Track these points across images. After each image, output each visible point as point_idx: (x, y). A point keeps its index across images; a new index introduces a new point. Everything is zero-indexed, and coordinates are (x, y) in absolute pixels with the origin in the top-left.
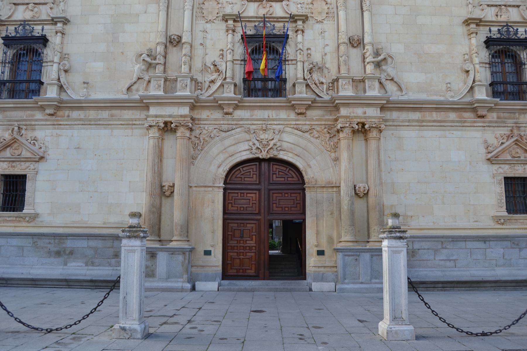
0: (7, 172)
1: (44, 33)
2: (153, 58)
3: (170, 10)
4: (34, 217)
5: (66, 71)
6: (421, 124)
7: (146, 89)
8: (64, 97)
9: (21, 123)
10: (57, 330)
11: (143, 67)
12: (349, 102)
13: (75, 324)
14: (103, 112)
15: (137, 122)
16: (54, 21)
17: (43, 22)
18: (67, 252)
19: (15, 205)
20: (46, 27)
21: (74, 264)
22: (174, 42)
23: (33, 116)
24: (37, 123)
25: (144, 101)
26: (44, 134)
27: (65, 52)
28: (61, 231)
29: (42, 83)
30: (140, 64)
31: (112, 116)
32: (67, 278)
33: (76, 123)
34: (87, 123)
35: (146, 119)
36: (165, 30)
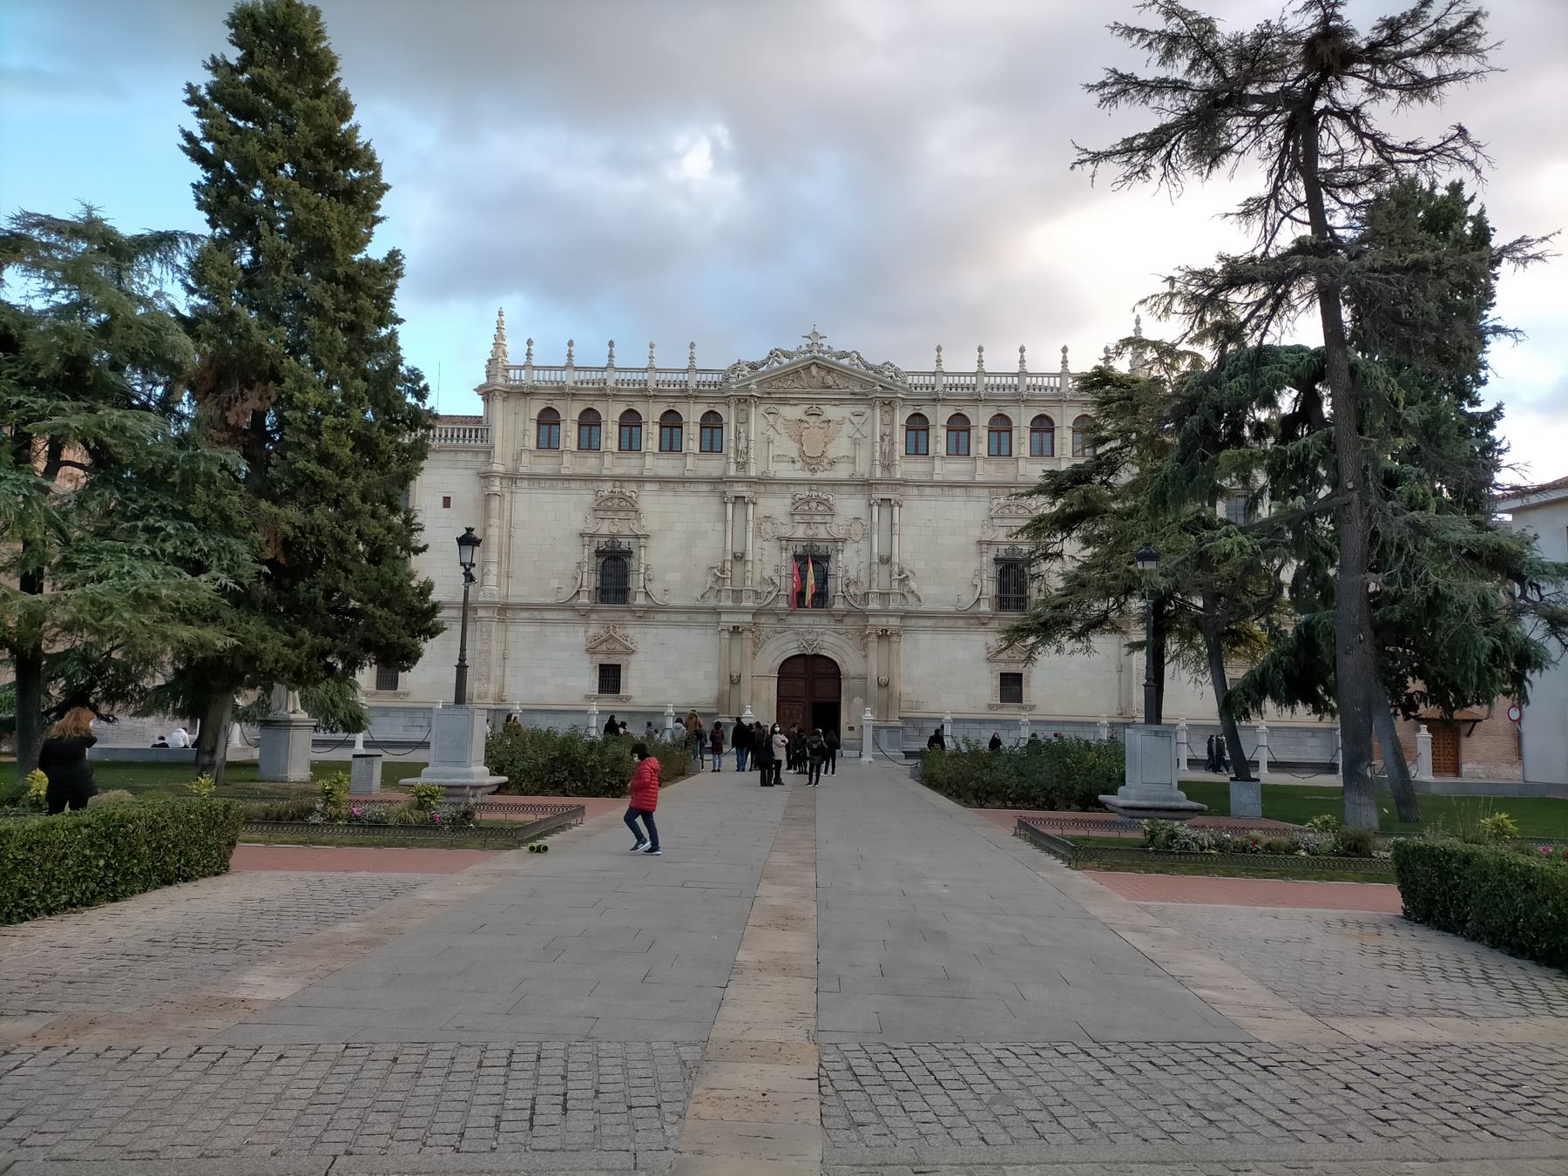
4: (628, 698)
6: (934, 629)
12: (875, 614)
22: (739, 558)
26: (634, 633)
34: (669, 624)
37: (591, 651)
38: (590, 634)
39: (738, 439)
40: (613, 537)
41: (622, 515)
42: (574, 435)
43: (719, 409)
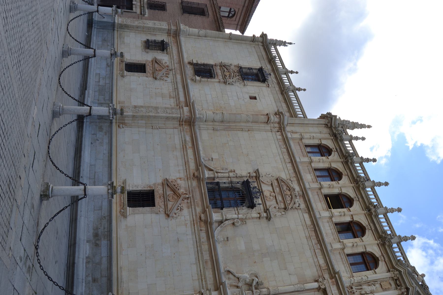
0: (156, 194)
1: (257, 205)
2: (257, 286)
3: (296, 293)
4: (124, 215)
5: (233, 224)
7: (231, 286)
8: (215, 225)
9: (192, 199)
10: (37, 253)
11: (248, 280)
13: (41, 266)
14: (208, 255)
15: (204, 283)
16: (266, 210)
17: (264, 204)
18: (97, 242)
19: (132, 201)
20: (261, 206)
21: (88, 247)
23: (198, 206)
24: (193, 209)
25: (221, 286)
26: (186, 215)
27: (247, 221)
28: (114, 235)
29: (222, 209)
30: (250, 277)
31: (206, 262)
32: (77, 245)
33: (197, 236)
34: (198, 244)
35: (207, 290)
36: (280, 292)
37: (166, 183)
38: (179, 181)
39: (369, 283)
40: (261, 192)
41: (280, 198)
42: (321, 165)
43: (382, 266)
